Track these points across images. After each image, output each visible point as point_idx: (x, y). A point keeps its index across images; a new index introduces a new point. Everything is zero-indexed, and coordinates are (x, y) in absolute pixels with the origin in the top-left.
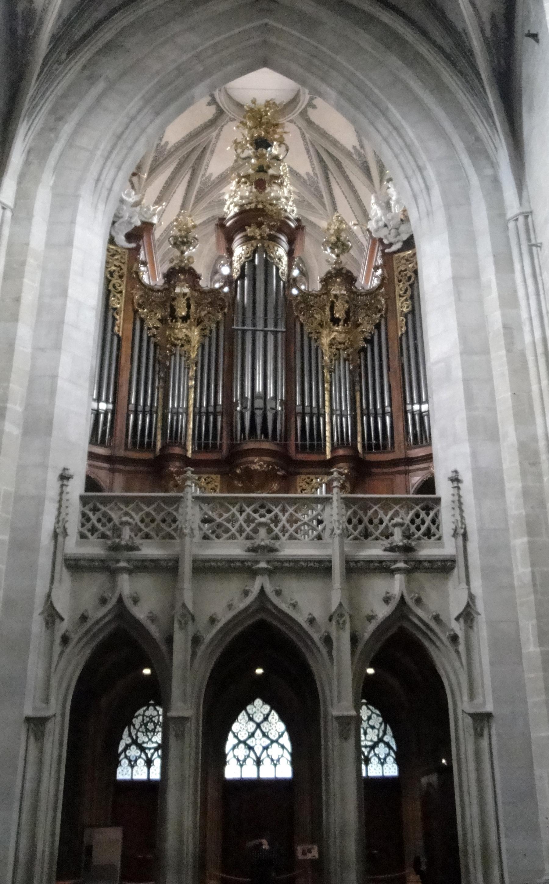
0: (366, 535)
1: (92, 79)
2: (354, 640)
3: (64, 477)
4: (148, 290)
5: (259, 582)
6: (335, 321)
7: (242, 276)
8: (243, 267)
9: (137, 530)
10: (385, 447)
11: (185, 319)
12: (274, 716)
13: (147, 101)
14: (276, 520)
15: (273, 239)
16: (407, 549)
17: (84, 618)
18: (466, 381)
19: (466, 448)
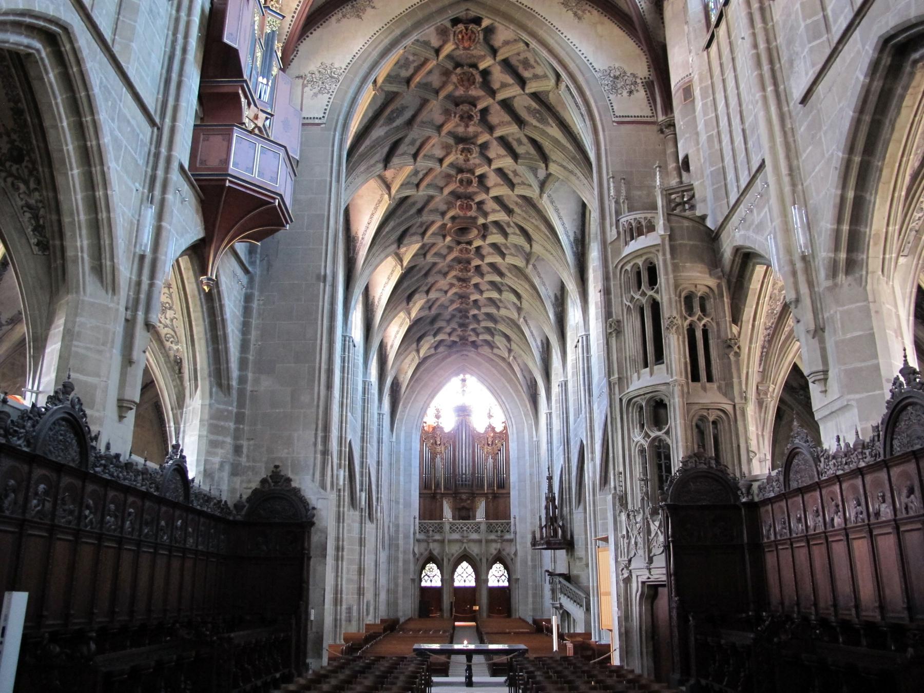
0: (491, 532)
1: (413, 392)
2: (487, 560)
3: (415, 518)
4: (427, 433)
5: (465, 545)
6: (488, 445)
7: (458, 429)
8: (458, 426)
9: (433, 531)
10: (504, 487)
11: (440, 445)
12: (470, 567)
13: (429, 395)
14: (468, 528)
15: (468, 415)
16: (502, 536)
17: (421, 554)
18: (519, 490)
19: (517, 510)
